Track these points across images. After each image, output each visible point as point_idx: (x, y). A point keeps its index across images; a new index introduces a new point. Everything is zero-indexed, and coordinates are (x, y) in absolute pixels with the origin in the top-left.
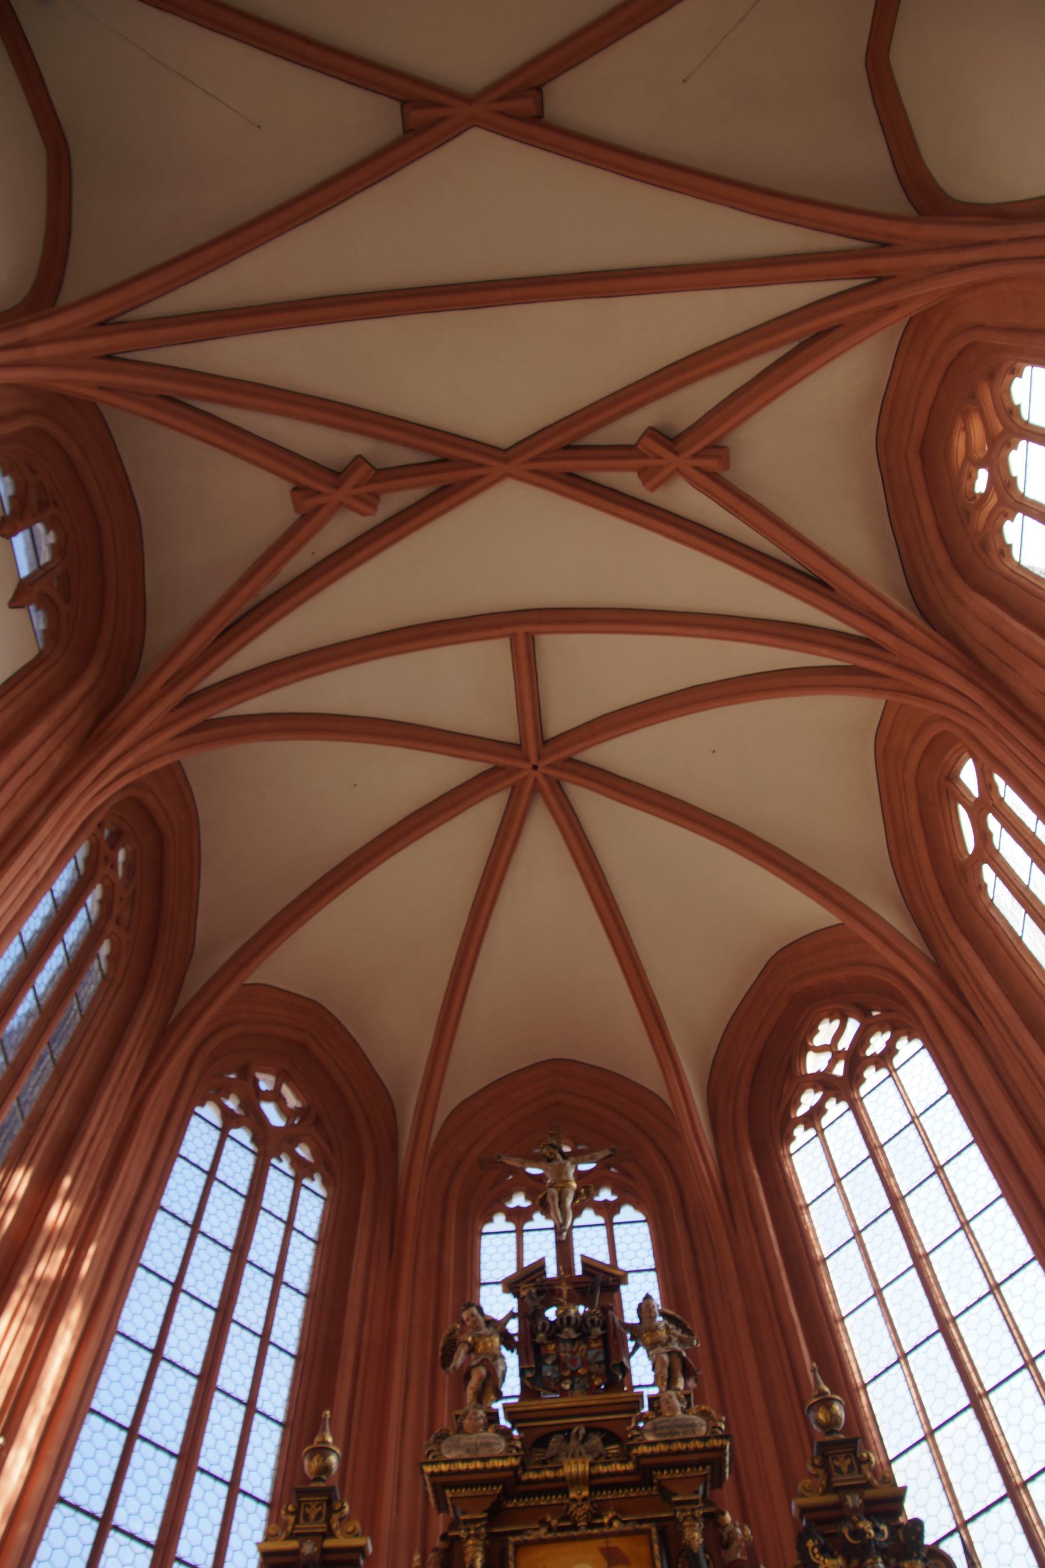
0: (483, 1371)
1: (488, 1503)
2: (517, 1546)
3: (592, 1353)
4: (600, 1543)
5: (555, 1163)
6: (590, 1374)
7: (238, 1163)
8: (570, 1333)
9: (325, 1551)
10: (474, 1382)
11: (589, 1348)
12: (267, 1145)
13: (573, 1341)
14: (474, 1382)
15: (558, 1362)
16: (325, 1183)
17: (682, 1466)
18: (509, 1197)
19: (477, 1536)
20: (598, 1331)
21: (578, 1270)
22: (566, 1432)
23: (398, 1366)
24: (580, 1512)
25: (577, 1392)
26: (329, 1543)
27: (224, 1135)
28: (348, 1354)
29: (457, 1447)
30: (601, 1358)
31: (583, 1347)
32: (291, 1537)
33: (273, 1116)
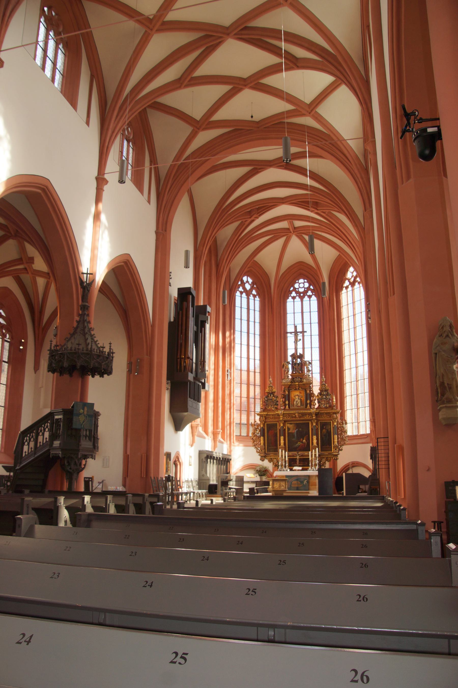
8: (297, 365)
12: (248, 293)
18: (291, 293)
24: (297, 388)
28: (267, 335)
33: (248, 287)
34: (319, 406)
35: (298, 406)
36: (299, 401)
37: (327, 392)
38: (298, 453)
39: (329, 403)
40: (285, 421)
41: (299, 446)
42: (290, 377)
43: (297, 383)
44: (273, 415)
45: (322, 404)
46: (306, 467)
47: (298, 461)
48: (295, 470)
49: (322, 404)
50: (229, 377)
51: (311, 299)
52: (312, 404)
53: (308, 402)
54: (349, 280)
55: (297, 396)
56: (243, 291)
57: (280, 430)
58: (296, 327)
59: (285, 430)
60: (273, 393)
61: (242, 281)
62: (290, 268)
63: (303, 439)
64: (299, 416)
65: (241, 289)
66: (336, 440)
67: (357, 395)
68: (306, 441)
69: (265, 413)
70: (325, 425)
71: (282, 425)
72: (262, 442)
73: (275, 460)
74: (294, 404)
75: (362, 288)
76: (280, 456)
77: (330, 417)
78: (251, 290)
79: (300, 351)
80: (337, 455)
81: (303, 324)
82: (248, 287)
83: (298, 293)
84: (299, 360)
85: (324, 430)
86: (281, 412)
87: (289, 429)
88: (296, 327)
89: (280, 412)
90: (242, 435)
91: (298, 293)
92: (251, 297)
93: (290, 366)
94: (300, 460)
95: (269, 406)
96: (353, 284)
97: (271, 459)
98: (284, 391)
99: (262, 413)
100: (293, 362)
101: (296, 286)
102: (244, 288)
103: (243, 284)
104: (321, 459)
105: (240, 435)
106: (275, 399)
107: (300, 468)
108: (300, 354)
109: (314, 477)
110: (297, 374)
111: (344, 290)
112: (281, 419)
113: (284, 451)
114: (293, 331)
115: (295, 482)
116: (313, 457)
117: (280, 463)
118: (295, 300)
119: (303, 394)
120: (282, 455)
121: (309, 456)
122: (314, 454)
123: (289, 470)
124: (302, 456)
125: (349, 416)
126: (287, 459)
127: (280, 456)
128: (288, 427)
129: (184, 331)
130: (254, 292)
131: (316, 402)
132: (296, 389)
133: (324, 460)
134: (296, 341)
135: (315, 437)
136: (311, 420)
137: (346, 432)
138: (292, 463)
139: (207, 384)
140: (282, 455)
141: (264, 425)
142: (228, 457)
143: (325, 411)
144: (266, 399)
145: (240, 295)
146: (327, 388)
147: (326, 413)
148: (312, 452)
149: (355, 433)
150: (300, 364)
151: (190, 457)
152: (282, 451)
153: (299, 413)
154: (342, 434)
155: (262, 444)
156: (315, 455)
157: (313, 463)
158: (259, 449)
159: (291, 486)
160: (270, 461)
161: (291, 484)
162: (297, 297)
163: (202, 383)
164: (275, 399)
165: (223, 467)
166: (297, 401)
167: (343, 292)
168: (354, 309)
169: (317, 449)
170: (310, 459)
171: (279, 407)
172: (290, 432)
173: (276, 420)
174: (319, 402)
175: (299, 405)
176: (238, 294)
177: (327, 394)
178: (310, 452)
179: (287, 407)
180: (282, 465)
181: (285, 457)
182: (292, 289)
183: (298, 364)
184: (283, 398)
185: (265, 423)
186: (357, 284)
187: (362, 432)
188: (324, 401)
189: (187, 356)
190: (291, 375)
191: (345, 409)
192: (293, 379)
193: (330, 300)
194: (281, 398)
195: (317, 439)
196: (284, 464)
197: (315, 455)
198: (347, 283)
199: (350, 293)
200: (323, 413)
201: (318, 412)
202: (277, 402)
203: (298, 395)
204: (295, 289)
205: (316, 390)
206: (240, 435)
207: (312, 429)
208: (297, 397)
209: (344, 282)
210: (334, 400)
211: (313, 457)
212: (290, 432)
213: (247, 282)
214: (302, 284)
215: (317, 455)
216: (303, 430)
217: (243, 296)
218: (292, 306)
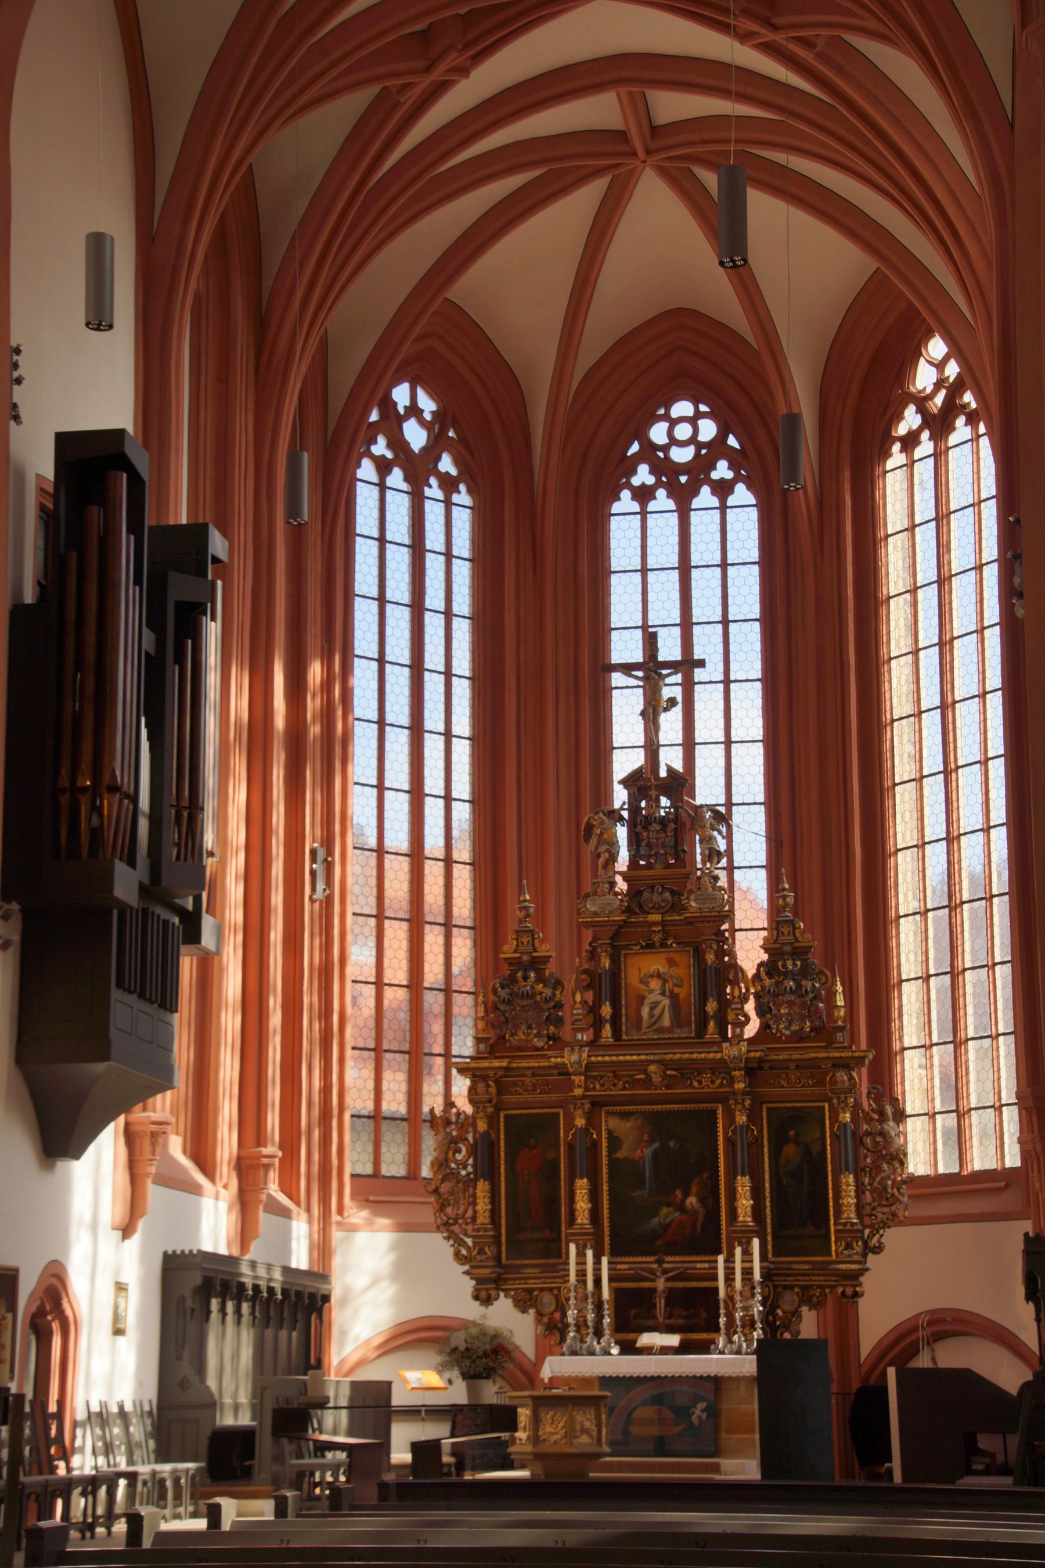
0: (607, 855)
1: (610, 935)
2: (625, 955)
3: (668, 839)
4: (666, 955)
5: (652, 682)
6: (666, 853)
7: (399, 506)
9: (533, 958)
10: (601, 861)
11: (667, 836)
12: (418, 469)
13: (658, 831)
14: (601, 861)
15: (649, 845)
16: (470, 491)
17: (709, 922)
19: (606, 951)
20: (673, 826)
21: (663, 773)
22: (652, 887)
23: (550, 687)
24: (657, 938)
25: (658, 866)
26: (535, 954)
27: (382, 487)
28: (511, 681)
29: (595, 905)
30: (672, 843)
31: (663, 835)
32: (515, 952)
33: (415, 436)
34: (764, 1027)
35: (661, 1030)
36: (666, 1002)
37: (804, 961)
38: (660, 1262)
39: (812, 1013)
40: (597, 1104)
41: (666, 1227)
42: (622, 885)
43: (656, 917)
44: (535, 1072)
45: (778, 1018)
46: (704, 1336)
47: (661, 1303)
48: (648, 1350)
49: (778, 1018)
50: (320, 885)
51: (731, 501)
52: (731, 1017)
53: (711, 1006)
54: (921, 402)
55: (653, 978)
56: (389, 455)
57: (570, 1147)
58: (650, 641)
59: (595, 1146)
60: (537, 964)
61: (387, 405)
62: (628, 344)
63: (687, 1194)
64: (665, 1076)
65: (380, 448)
66: (850, 1200)
67: (955, 974)
68: (701, 1200)
69: (496, 1063)
70: (790, 1125)
71: (580, 1122)
72: (483, 1206)
73: (547, 1299)
74: (640, 1018)
75: (985, 443)
76: (573, 1278)
77: (821, 1082)
78: (432, 451)
79: (671, 759)
80: (854, 1277)
81: (686, 625)
82: (415, 436)
83: (664, 468)
84: (664, 801)
85: (790, 1150)
86: (574, 1057)
87: (615, 1143)
88: (650, 641)
89: (570, 1058)
90: (385, 1171)
91: (664, 468)
92: (434, 490)
93: (622, 833)
94: (672, 1296)
95: (516, 1027)
96: (939, 425)
97: (529, 1291)
98: (593, 955)
99: (485, 1064)
100: (634, 809)
101: (658, 433)
102: (398, 443)
103: (392, 422)
104: (777, 1296)
105: (376, 1174)
106: (548, 992)
107: (673, 1340)
108: (670, 770)
109: (743, 1387)
110: (658, 870)
111: (897, 457)
112: (578, 1092)
113: (590, 1253)
114: (638, 657)
115: (648, 1412)
116: (738, 1284)
117: (571, 1315)
118: (652, 506)
119: (684, 969)
120: (582, 1274)
121: (715, 1278)
122: (739, 1269)
123: (615, 1351)
124: (682, 1277)
125: (917, 1080)
126: (606, 1294)
127: (573, 1278)
128: (610, 1133)
129: (90, 654)
130: (446, 464)
131: (750, 1007)
132: (650, 946)
133: (789, 1300)
134: (651, 714)
135: (743, 1185)
136: (722, 1099)
137: (899, 1158)
138: (631, 1314)
139: (208, 923)
140: (582, 1274)
141: (492, 1121)
142: (311, 1285)
143: (796, 1056)
144: (503, 993)
145: (374, 477)
146: (806, 939)
147: (800, 1065)
148: (730, 1259)
149: (946, 1166)
150: (672, 819)
151: (121, 1288)
152: (581, 1254)
153: (664, 1064)
154: (879, 1169)
155: (483, 1218)
156: (747, 1272)
157: (738, 1315)
158: (469, 1241)
159: (626, 1433)
160: (522, 1304)
161: (629, 1421)
162: (661, 493)
163: (182, 912)
164: (548, 992)
165: (289, 1338)
166: (654, 1005)
167: (890, 464)
168: (943, 547)
169: (756, 1242)
170: (722, 1294)
171: (566, 1033)
172: (621, 1154)
173: (554, 1097)
174: (761, 1011)
175: (666, 1022)
176: (367, 470)
177: (806, 972)
178: (721, 1259)
179: (607, 1030)
180: (581, 1325)
181: (598, 1281)
182: (635, 448)
183: (663, 822)
184: (589, 987)
185: (498, 1109)
186: (960, 421)
187: (981, 1160)
188: (791, 1004)
189: (106, 780)
190: (626, 877)
191: (896, 1046)
192: (634, 892)
193: (826, 506)
194: (577, 988)
195: (756, 1193)
196: (591, 1317)
197: (747, 1272)
198: (910, 419)
199: (924, 471)
200: (782, 1067)
201: (760, 1060)
202: (559, 1006)
203: (659, 975)
204: (649, 452)
205: (750, 953)
206: (376, 1174)
207: (730, 1144)
208: (655, 984)
209: (899, 417)
210: (840, 1001)
211: (738, 1284)
212: (621, 1154)
213: (414, 410)
214: (683, 427)
215: (757, 1276)
216: (684, 1148)
217: (390, 481)
218: (635, 534)
